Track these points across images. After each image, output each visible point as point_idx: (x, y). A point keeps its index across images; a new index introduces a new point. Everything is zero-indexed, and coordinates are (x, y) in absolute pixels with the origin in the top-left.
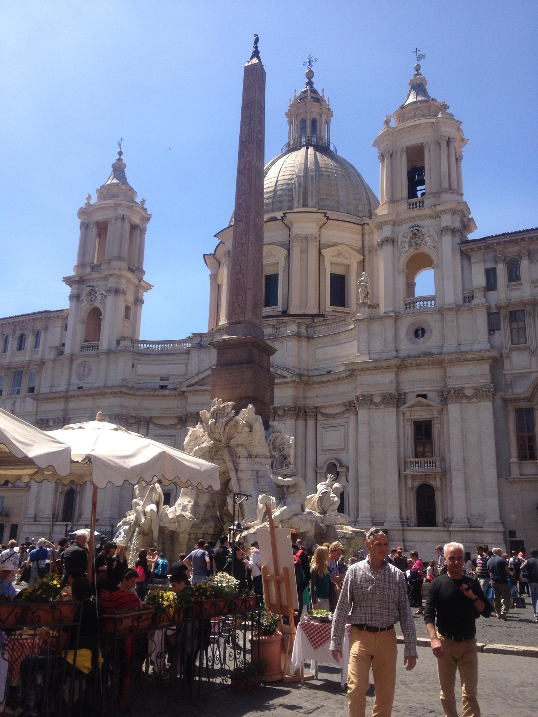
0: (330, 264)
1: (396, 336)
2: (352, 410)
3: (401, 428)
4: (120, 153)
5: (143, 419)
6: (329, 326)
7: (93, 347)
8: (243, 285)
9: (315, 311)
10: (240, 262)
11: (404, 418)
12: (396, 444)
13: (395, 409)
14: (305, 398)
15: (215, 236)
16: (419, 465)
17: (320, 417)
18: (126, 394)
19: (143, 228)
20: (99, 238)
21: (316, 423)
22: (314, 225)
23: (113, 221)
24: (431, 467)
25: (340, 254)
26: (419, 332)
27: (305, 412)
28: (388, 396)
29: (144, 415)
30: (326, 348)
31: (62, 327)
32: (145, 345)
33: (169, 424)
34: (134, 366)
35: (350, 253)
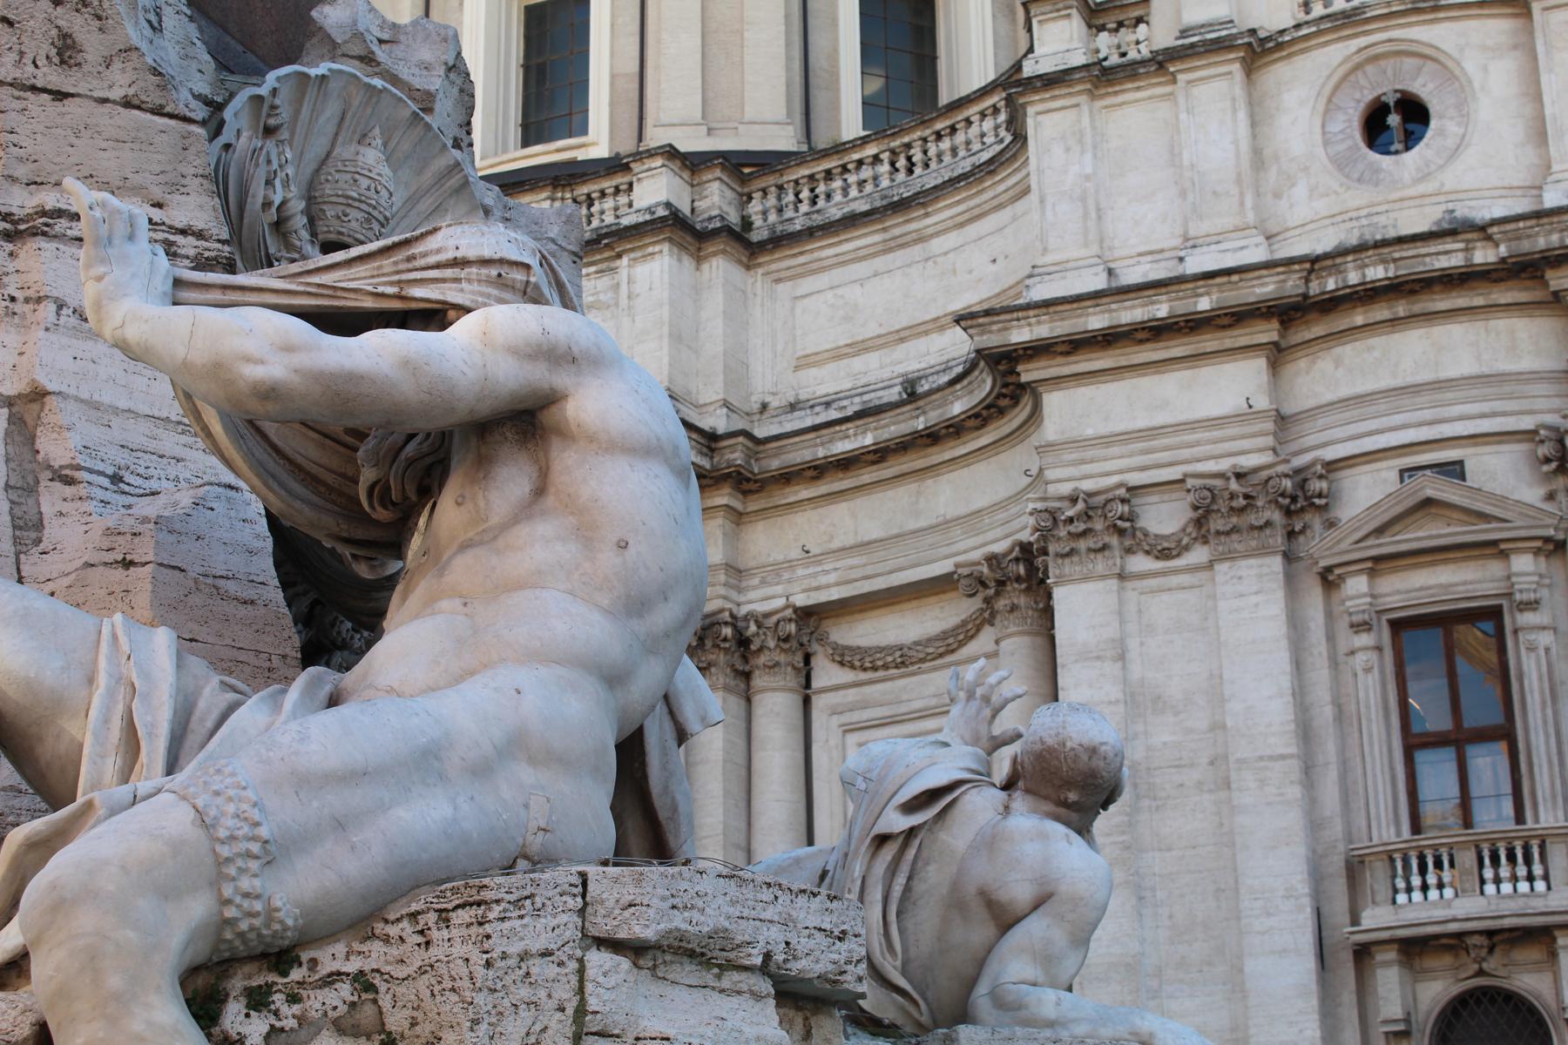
1: (1259, 159)
2: (1014, 608)
3: (1320, 676)
6: (866, 172)
9: (785, 139)
11: (1329, 616)
12: (1294, 765)
13: (1276, 563)
14: (736, 572)
16: (1447, 876)
17: (826, 673)
21: (807, 701)
24: (1523, 887)
26: (1394, 120)
27: (743, 642)
28: (1234, 485)
30: (854, 293)
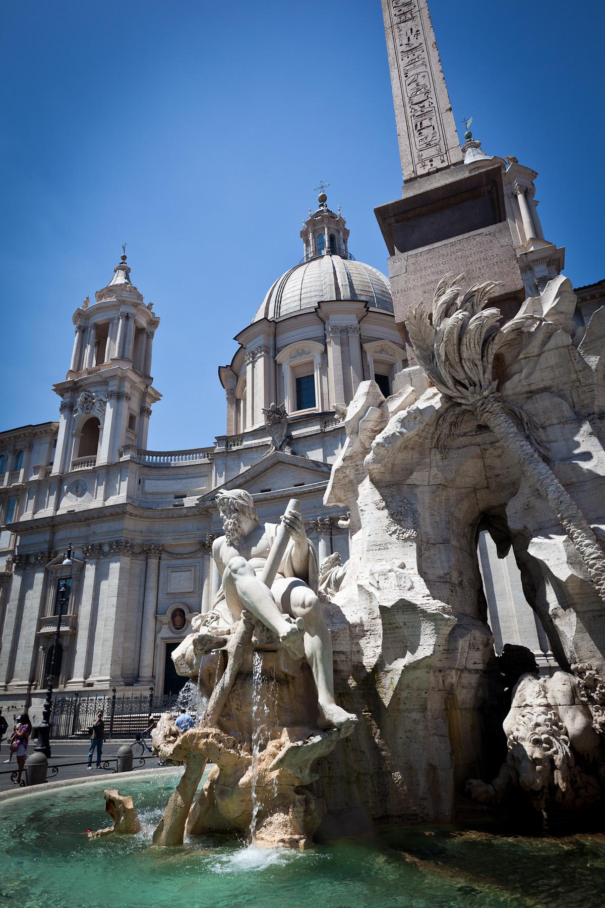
0: (374, 361)
4: (124, 258)
5: (153, 547)
7: (88, 462)
8: (430, 109)
10: (412, 78)
15: (235, 339)
18: (131, 514)
19: (150, 333)
20: (99, 346)
22: (354, 317)
23: (115, 321)
25: (382, 350)
29: (154, 542)
31: (51, 443)
32: (154, 457)
33: (186, 552)
34: (141, 482)
35: (394, 350)
